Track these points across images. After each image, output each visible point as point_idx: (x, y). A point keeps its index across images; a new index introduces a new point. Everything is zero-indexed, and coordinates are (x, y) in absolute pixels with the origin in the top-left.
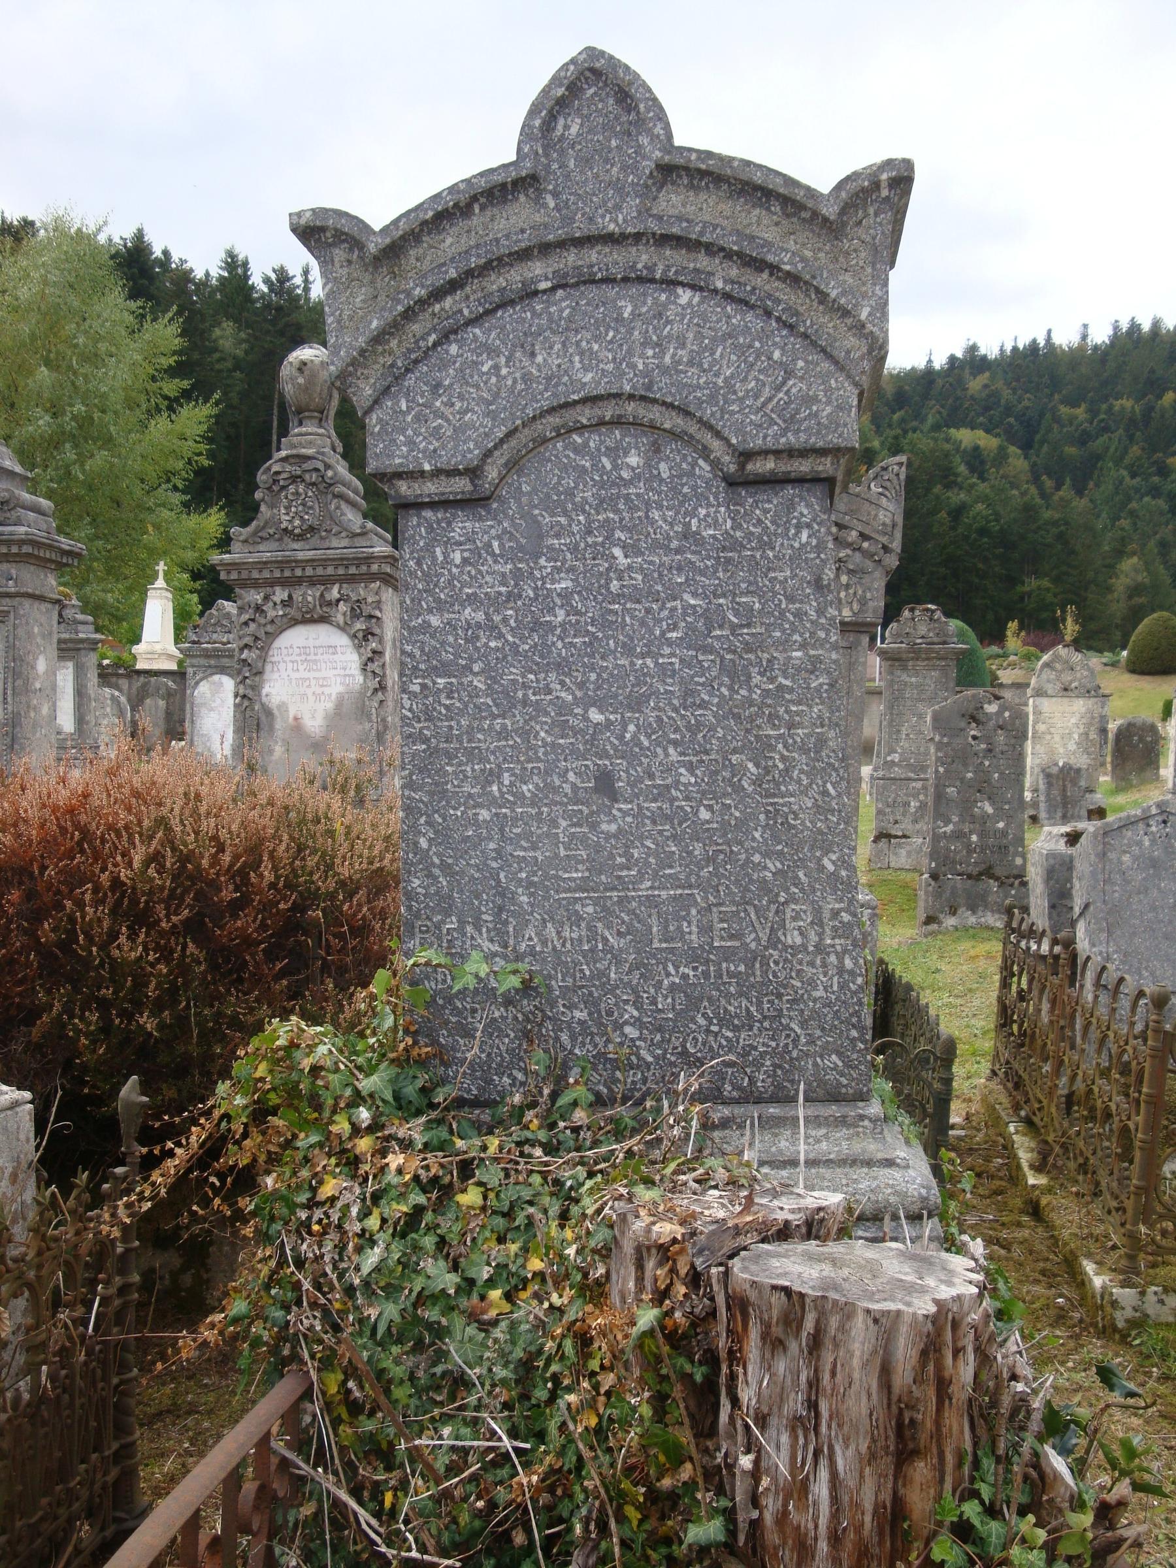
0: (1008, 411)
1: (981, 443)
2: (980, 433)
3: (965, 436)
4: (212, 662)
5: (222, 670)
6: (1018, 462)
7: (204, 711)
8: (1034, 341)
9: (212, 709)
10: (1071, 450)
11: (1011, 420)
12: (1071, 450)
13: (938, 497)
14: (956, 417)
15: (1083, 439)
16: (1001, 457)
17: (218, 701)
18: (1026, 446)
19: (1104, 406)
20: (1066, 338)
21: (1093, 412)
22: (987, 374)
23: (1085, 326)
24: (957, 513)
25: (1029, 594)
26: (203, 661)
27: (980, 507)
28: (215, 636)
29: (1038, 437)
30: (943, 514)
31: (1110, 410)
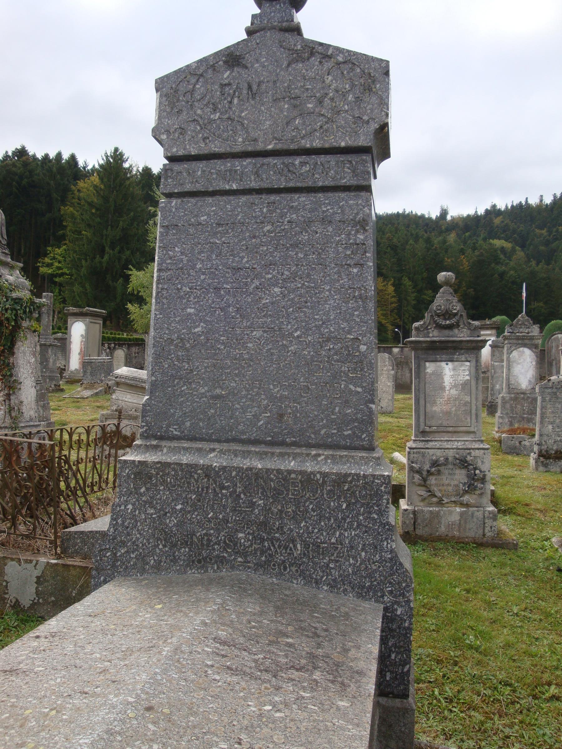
0: (514, 231)
1: (505, 245)
2: (503, 241)
3: (498, 243)
4: (520, 342)
5: (525, 345)
6: (520, 254)
7: (515, 364)
8: (521, 202)
9: (519, 364)
10: (542, 248)
11: (515, 235)
12: (542, 248)
13: (493, 269)
14: (493, 233)
15: (547, 243)
16: (513, 250)
17: (522, 360)
18: (523, 246)
19: (555, 229)
20: (534, 201)
21: (550, 232)
22: (501, 217)
23: (542, 196)
24: (502, 275)
25: (534, 309)
26: (515, 341)
27: (512, 272)
28: (521, 330)
29: (528, 243)
30: (496, 276)
31: (557, 231)
